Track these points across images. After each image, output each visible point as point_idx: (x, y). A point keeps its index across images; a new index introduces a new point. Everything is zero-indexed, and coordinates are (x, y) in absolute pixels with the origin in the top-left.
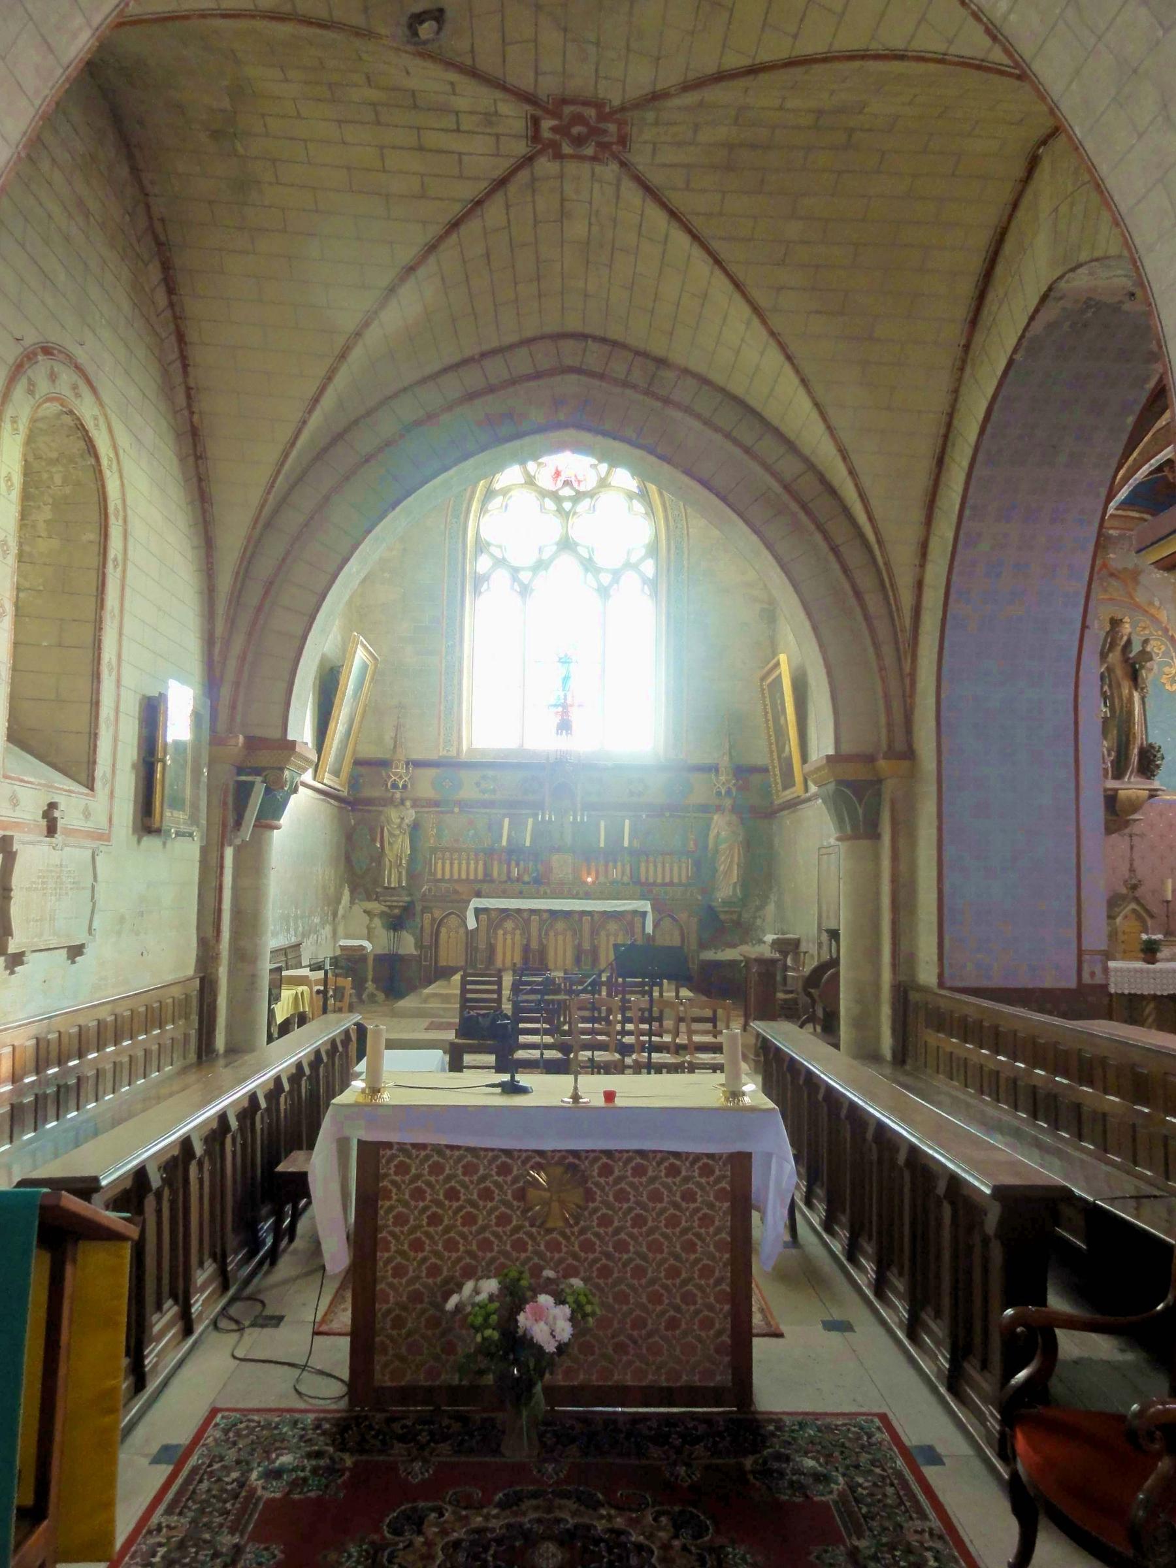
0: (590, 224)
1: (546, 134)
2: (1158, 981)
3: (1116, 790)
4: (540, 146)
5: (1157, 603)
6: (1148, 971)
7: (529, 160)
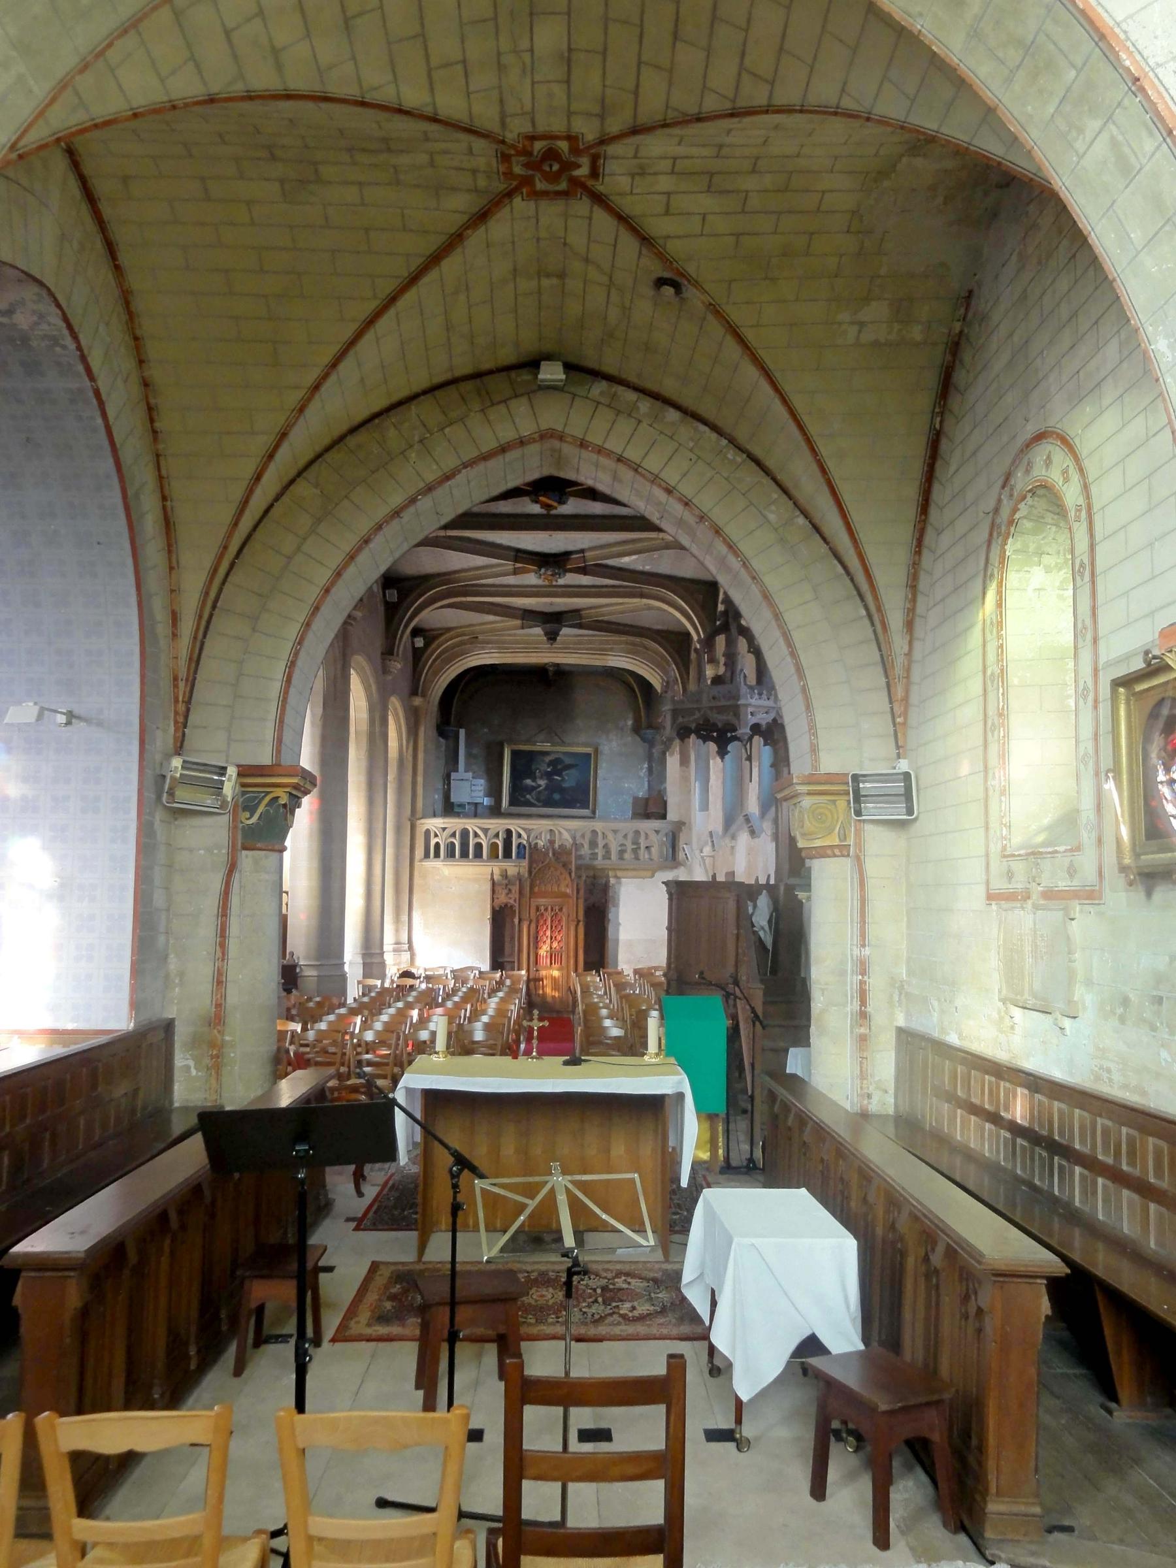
0: (532, 50)
1: (585, 161)
4: (593, 151)
7: (603, 141)
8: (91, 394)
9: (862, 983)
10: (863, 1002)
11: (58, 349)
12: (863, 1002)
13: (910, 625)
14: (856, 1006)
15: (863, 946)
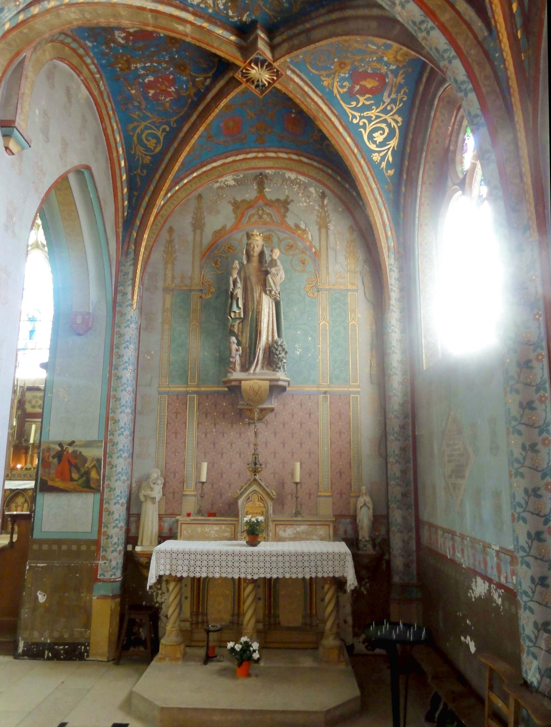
2: (250, 564)
3: (240, 381)
5: (303, 226)
6: (246, 555)
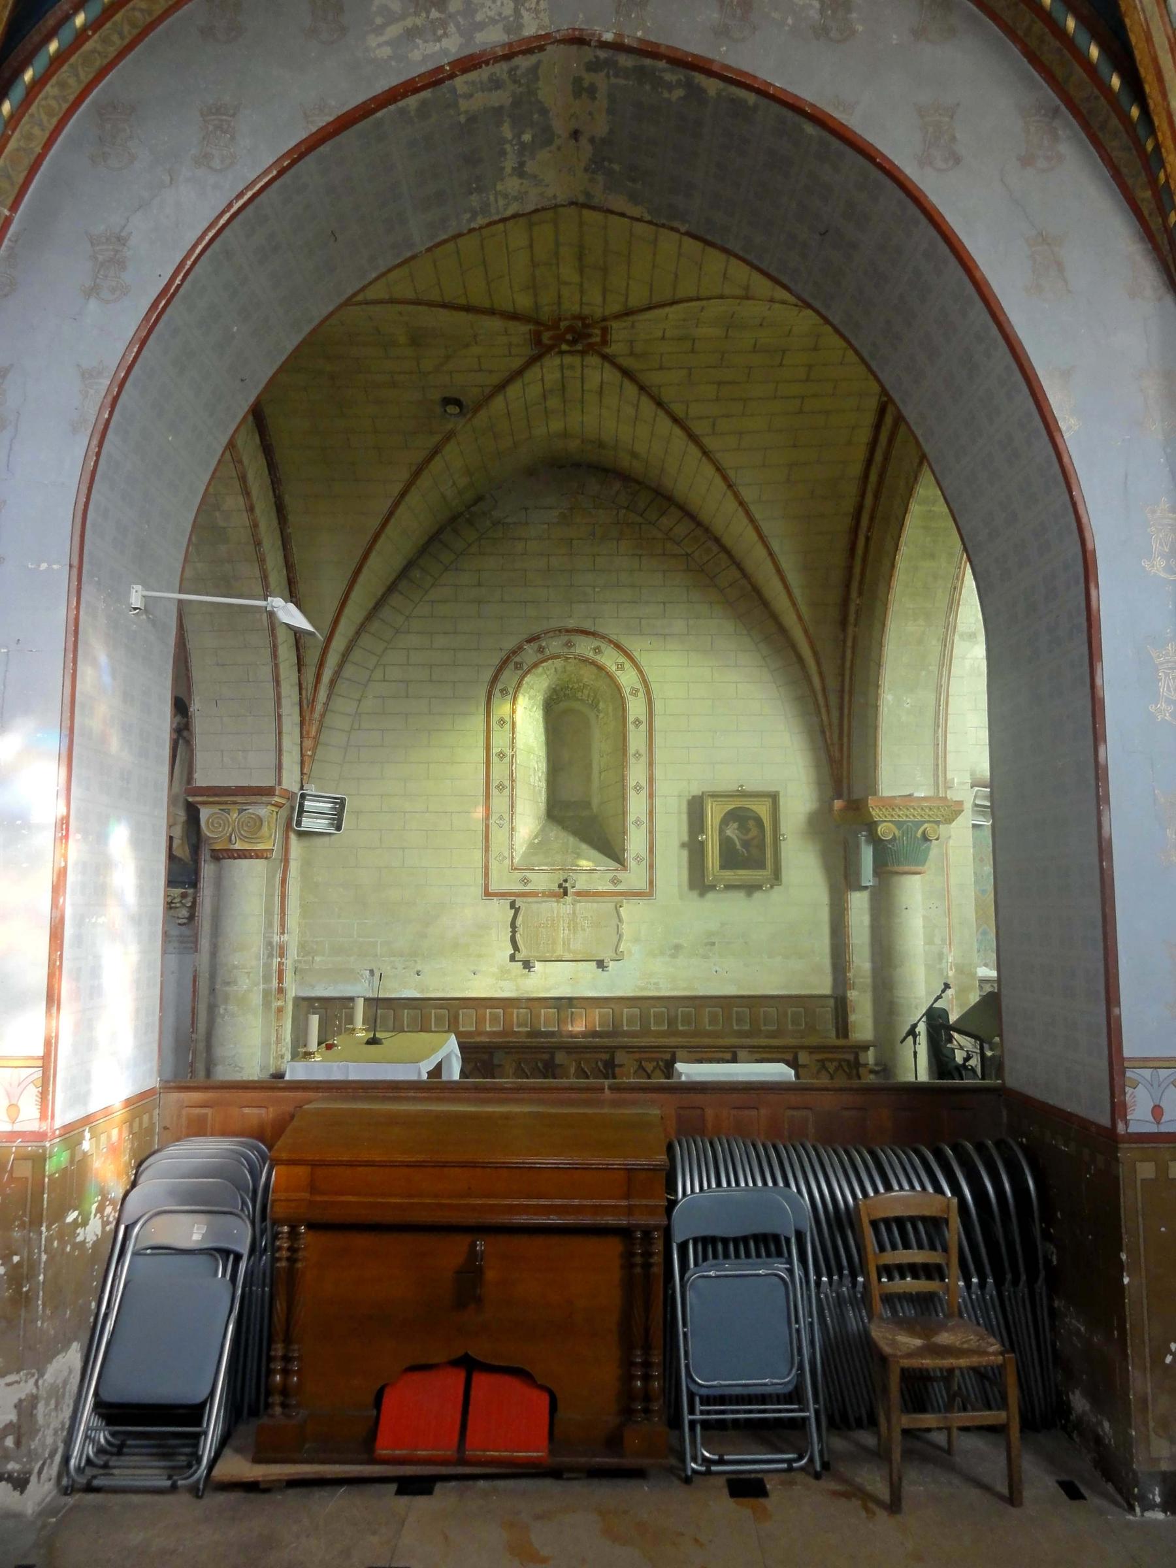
8: (409, 254)
9: (281, 964)
10: (281, 980)
11: (468, 216)
12: (281, 980)
13: (333, 683)
14: (275, 983)
15: (283, 933)
